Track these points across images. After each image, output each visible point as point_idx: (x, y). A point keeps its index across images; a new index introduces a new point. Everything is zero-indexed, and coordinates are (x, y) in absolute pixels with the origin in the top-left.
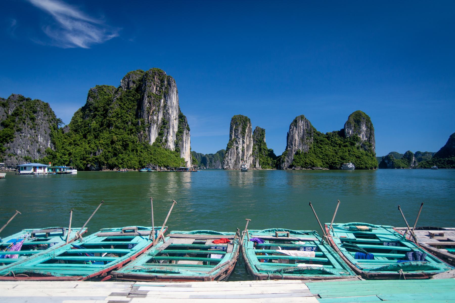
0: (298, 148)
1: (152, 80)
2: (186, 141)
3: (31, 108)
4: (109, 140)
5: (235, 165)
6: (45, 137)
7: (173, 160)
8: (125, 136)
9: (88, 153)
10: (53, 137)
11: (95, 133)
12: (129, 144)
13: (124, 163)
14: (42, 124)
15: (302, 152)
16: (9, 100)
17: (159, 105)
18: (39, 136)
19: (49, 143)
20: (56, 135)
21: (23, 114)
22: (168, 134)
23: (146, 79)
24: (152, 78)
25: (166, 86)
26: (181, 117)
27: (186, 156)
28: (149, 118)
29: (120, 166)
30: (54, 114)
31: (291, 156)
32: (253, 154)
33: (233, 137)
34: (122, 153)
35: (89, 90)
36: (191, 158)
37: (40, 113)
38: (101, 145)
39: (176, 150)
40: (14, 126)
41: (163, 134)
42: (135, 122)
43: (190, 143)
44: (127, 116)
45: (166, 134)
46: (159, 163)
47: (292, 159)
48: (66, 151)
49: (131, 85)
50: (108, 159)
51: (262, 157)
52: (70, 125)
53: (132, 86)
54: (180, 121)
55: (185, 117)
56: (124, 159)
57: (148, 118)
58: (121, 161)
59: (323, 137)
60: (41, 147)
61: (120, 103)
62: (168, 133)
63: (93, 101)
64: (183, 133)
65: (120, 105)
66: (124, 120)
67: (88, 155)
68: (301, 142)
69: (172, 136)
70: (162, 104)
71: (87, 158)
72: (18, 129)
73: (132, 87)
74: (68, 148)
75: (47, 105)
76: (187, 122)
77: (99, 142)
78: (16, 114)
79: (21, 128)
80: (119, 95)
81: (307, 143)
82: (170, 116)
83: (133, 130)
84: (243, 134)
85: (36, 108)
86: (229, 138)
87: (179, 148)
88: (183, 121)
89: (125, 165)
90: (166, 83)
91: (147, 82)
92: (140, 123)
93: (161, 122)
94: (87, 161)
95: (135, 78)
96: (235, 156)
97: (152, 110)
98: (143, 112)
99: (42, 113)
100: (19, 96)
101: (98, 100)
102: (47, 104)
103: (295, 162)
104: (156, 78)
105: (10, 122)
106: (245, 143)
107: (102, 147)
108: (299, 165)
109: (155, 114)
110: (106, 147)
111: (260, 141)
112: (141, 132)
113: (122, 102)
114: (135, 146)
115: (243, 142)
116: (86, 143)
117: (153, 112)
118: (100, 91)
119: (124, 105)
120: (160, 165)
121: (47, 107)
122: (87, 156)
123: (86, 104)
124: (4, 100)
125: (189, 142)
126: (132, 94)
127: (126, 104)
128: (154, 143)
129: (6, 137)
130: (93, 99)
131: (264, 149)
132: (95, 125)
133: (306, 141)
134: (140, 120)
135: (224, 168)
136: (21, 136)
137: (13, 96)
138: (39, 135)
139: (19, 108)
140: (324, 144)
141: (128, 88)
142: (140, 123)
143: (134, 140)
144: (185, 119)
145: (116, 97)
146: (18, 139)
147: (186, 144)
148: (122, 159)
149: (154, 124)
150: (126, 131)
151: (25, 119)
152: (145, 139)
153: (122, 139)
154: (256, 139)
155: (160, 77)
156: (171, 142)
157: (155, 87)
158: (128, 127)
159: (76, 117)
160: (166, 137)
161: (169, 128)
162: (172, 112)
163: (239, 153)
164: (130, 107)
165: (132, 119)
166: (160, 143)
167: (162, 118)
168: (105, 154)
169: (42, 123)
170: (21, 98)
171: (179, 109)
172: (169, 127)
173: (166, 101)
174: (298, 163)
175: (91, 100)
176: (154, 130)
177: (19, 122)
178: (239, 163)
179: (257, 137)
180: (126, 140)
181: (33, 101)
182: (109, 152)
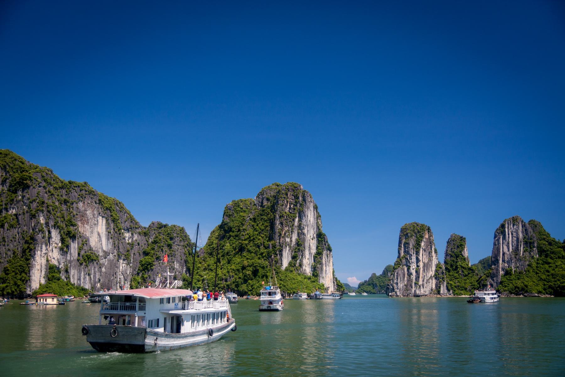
0: (508, 264)
1: (284, 198)
2: (326, 264)
3: (168, 234)
4: (240, 265)
5: (405, 290)
6: (181, 263)
7: (305, 286)
8: (255, 261)
9: (220, 279)
10: (188, 262)
11: (228, 257)
12: (258, 270)
13: (254, 290)
14: (178, 250)
15: (515, 271)
16: (150, 228)
17: (293, 225)
18: (175, 263)
19: (185, 269)
20: (191, 260)
21: (161, 241)
22: (303, 257)
23: (278, 197)
24: (285, 196)
25: (301, 202)
26: (320, 237)
27: (327, 280)
28: (281, 240)
29: (249, 293)
30: (189, 239)
31: (497, 276)
32: (435, 275)
33: (402, 254)
34: (252, 280)
35: (225, 206)
36: (334, 283)
37: (176, 239)
38: (232, 270)
39: (313, 275)
40: (154, 254)
41: (297, 257)
42: (267, 245)
43: (333, 265)
44: (259, 239)
45: (301, 257)
46: (288, 290)
47: (498, 280)
48: (200, 277)
49: (265, 203)
50: (239, 286)
51: (457, 278)
52: (205, 248)
53: (265, 204)
54: (318, 240)
55: (325, 235)
56: (253, 286)
57: (280, 241)
58: (250, 288)
59: (558, 247)
60: (177, 273)
61: (253, 224)
62: (302, 256)
63: (228, 220)
64: (322, 255)
65: (253, 226)
66: (256, 243)
67: (220, 282)
68: (513, 256)
69: (308, 259)
70: (296, 224)
71: (219, 284)
72: (157, 256)
73: (266, 205)
74: (203, 273)
75: (183, 230)
76: (327, 242)
77: (230, 267)
78: (155, 242)
79: (160, 255)
80: (252, 214)
81: (525, 258)
82: (305, 235)
83: (264, 254)
84: (417, 248)
85: (172, 234)
86: (397, 255)
87: (318, 273)
88: (322, 241)
89: (254, 292)
90: (301, 198)
91: (280, 200)
92: (271, 246)
93: (295, 243)
94: (219, 288)
95: (270, 194)
96: (406, 279)
97: (284, 231)
98: (275, 234)
99: (178, 238)
100: (158, 223)
101: (233, 219)
102: (183, 228)
103: (502, 285)
104: (289, 195)
105: (150, 250)
106: (421, 261)
107: (233, 273)
108: (506, 290)
109: (287, 236)
110: (237, 273)
111: (455, 255)
112: (272, 256)
113: (255, 222)
114: (265, 272)
115: (418, 260)
116: (219, 268)
117: (285, 234)
118: (235, 207)
119: (257, 225)
120: (289, 291)
121: (183, 232)
122: (219, 282)
123: (222, 223)
124: (145, 229)
125: (331, 264)
126: (266, 213)
127: (259, 225)
128: (286, 267)
129: (148, 265)
130: (229, 217)
131: (462, 267)
132: (228, 248)
133: (523, 255)
134: (270, 243)
135: (389, 294)
136: (159, 263)
137: (153, 224)
138: (176, 261)
139: (158, 235)
140: (556, 258)
141: (262, 206)
142: (271, 246)
143: (264, 265)
144: (324, 238)
145: (249, 217)
146: (156, 266)
147: (326, 266)
148: (252, 286)
149: (286, 247)
150: (257, 255)
151: (163, 246)
152: (276, 264)
153: (252, 264)
154: (451, 253)
155: (295, 192)
156: (307, 265)
157: (289, 204)
158: (260, 250)
159: (212, 237)
160: (301, 260)
161: (304, 250)
162: (308, 231)
163: (411, 274)
164: (263, 228)
165: (265, 241)
166: (294, 267)
167: (296, 240)
168: (236, 280)
169: (178, 248)
170: (160, 225)
171: (318, 227)
172: (304, 248)
173: (300, 220)
174: (506, 287)
175: (227, 220)
176: (286, 253)
177: (158, 249)
178: (412, 287)
179: (452, 249)
180: (256, 266)
181: (170, 227)
182: (240, 278)
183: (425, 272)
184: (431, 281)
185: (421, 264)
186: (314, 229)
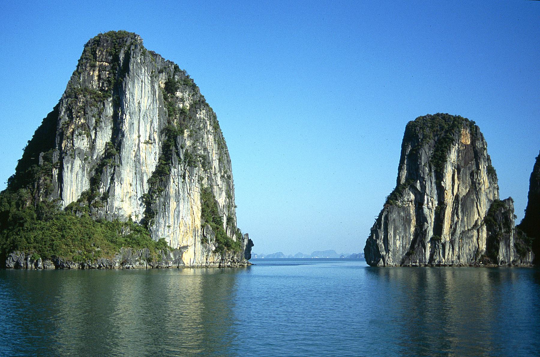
32: (486, 221)
156: (127, 199)
161: (118, 166)
183: (457, 214)
184: (475, 232)
185: (449, 199)
186: (152, 122)
